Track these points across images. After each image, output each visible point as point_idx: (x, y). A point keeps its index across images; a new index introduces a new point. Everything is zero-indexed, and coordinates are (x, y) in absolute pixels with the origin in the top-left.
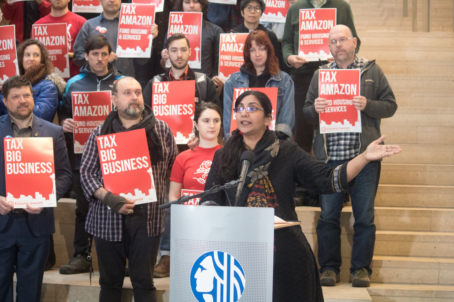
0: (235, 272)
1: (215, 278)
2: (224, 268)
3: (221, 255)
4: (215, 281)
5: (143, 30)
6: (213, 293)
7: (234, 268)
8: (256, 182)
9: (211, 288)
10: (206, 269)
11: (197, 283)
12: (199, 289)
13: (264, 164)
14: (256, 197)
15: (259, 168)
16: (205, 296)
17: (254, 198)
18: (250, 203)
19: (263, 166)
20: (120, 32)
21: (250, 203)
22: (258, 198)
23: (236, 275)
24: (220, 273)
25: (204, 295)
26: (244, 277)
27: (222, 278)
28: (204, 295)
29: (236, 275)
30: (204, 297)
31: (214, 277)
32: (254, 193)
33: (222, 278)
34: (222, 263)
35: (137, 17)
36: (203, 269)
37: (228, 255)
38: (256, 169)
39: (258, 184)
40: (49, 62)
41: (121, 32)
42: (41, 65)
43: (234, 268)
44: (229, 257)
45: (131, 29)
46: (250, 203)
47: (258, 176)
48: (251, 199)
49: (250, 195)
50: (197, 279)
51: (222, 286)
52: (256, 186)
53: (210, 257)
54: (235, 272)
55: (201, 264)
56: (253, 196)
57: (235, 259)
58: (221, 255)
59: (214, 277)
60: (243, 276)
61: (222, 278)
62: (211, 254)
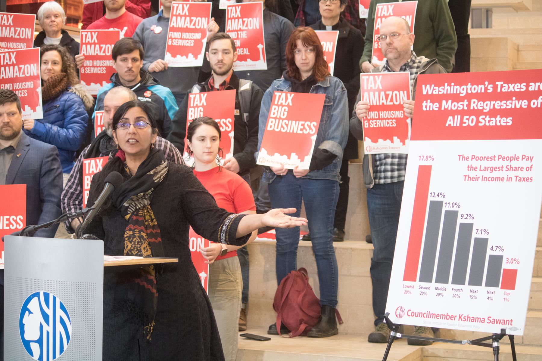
5: (196, 34)
8: (133, 212)
13: (145, 191)
14: (133, 231)
15: (137, 196)
17: (131, 233)
18: (127, 238)
19: (142, 194)
20: (170, 37)
21: (127, 238)
22: (136, 233)
32: (132, 226)
35: (242, 20)
38: (134, 197)
39: (137, 215)
40: (72, 71)
41: (171, 36)
42: (63, 74)
45: (183, 33)
46: (126, 239)
47: (136, 206)
48: (127, 233)
49: (127, 228)
52: (134, 218)
56: (130, 230)
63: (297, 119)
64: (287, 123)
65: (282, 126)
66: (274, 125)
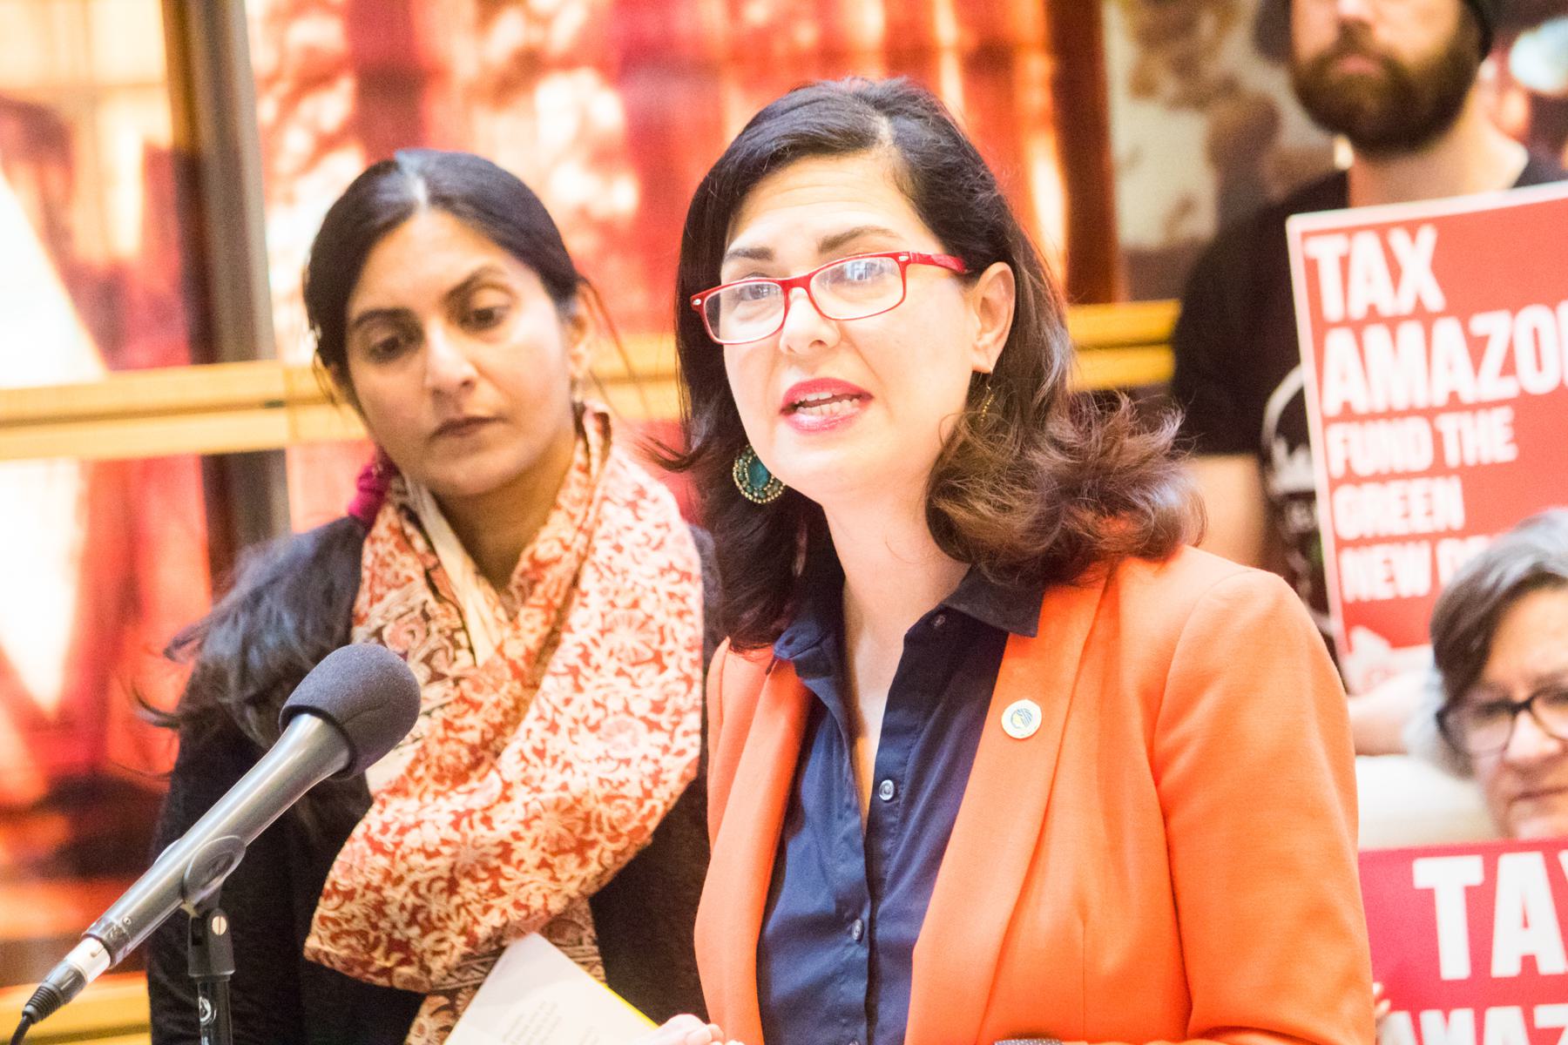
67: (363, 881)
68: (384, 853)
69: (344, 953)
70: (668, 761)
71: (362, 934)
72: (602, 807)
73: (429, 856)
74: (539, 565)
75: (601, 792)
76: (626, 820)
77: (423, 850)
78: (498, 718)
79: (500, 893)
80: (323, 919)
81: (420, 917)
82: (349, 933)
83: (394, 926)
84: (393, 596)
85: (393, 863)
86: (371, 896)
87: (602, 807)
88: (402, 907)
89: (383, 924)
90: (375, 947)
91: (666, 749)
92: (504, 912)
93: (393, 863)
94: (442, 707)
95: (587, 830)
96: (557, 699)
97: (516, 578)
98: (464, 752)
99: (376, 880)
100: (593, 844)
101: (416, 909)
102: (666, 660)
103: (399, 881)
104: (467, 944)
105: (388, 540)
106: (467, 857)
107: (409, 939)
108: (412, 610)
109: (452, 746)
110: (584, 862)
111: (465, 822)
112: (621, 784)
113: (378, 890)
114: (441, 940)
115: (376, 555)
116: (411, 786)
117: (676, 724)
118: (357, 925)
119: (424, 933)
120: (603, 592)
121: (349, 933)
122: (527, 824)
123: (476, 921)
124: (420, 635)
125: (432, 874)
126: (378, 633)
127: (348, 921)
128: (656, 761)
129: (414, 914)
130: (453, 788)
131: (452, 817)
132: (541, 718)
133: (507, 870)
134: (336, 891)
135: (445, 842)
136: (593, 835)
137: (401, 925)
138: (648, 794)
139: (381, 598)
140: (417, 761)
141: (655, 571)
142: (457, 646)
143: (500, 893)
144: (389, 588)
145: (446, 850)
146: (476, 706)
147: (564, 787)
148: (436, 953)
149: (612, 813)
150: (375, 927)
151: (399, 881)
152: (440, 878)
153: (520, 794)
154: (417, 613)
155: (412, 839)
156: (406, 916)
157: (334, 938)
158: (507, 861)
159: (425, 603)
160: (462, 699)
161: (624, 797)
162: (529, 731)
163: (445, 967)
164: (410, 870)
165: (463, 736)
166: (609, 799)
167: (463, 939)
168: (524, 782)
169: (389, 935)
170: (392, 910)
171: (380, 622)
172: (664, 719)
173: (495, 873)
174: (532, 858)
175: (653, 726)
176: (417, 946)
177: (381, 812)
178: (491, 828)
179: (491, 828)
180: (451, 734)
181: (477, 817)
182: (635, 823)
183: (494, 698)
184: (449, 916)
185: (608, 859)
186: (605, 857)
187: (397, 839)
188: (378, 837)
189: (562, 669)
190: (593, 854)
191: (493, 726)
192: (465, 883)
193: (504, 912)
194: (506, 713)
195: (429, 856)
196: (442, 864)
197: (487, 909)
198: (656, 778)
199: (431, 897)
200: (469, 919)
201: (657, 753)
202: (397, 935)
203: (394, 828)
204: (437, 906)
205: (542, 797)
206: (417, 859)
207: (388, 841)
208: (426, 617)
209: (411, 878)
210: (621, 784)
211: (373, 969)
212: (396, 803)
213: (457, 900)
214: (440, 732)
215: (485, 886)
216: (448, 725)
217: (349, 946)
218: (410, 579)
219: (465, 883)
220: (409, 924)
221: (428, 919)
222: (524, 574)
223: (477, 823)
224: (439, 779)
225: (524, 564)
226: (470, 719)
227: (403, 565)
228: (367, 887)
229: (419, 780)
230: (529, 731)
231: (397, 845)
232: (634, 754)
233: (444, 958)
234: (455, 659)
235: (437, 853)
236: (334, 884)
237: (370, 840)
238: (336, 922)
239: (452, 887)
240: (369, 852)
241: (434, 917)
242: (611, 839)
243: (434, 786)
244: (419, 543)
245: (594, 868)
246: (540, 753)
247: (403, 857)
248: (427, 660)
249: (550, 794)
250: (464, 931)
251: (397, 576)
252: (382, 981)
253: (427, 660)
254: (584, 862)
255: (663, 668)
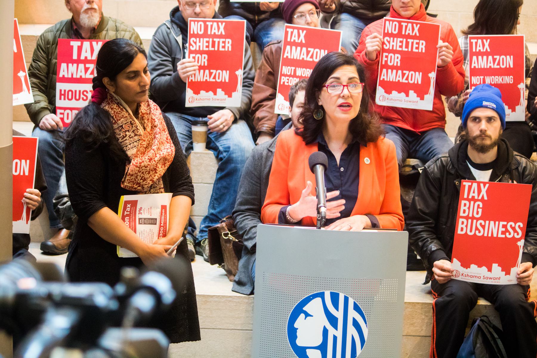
0: (354, 319)
1: (325, 327)
2: (339, 315)
3: (335, 298)
4: (325, 332)
6: (323, 348)
7: (352, 314)
9: (319, 341)
10: (312, 316)
11: (298, 334)
12: (300, 342)
16: (309, 352)
23: (356, 324)
24: (333, 321)
25: (308, 350)
26: (367, 326)
27: (336, 328)
28: (308, 350)
29: (356, 324)
30: (308, 354)
31: (325, 327)
33: (336, 328)
34: (336, 307)
36: (307, 315)
37: (345, 297)
43: (352, 314)
44: (346, 299)
50: (297, 329)
51: (335, 338)
53: (319, 300)
54: (354, 319)
55: (304, 309)
57: (354, 302)
58: (335, 298)
59: (325, 327)
60: (365, 325)
61: (335, 327)
62: (321, 295)
63: (496, 218)
64: (483, 223)
65: (477, 229)
66: (467, 226)
67: (134, 172)
68: (138, 167)
69: (130, 185)
70: (172, 148)
71: (133, 182)
72: (168, 157)
73: (146, 167)
74: (143, 114)
75: (167, 154)
76: (170, 159)
77: (144, 166)
78: (148, 143)
79: (157, 173)
80: (128, 180)
81: (143, 178)
82: (131, 182)
83: (138, 180)
84: (122, 119)
85: (140, 169)
86: (136, 175)
87: (168, 157)
88: (140, 176)
89: (137, 180)
90: (134, 184)
91: (171, 147)
92: (158, 176)
93: (140, 169)
94: (139, 140)
95: (165, 161)
96: (159, 138)
97: (140, 116)
98: (144, 149)
99: (137, 172)
100: (166, 163)
101: (143, 177)
102: (165, 130)
103: (140, 172)
104: (152, 182)
105: (118, 109)
106: (152, 167)
107: (140, 182)
108: (128, 122)
109: (142, 148)
110: (165, 167)
111: (151, 161)
112: (169, 152)
113: (137, 174)
114: (146, 182)
115: (115, 112)
116: (138, 156)
117: (170, 142)
118: (133, 180)
119: (143, 182)
120: (156, 118)
121: (131, 182)
122: (159, 161)
123: (153, 178)
124: (131, 127)
125: (146, 170)
126: (122, 126)
127: (131, 180)
128: (171, 148)
129: (142, 178)
130: (144, 155)
131: (148, 160)
132: (158, 142)
133: (157, 169)
134: (130, 175)
135: (149, 165)
136: (166, 162)
137: (139, 180)
138: (172, 154)
139: (120, 120)
140: (137, 151)
141: (159, 114)
142: (138, 129)
143: (157, 173)
144: (121, 118)
145: (149, 166)
146: (145, 141)
147: (163, 154)
148: (145, 185)
149: (168, 158)
150: (135, 180)
151: (140, 172)
152: (147, 171)
153: (158, 155)
154: (129, 123)
155: (143, 164)
156: (141, 178)
157: (129, 183)
158: (157, 167)
159: (131, 121)
160: (142, 139)
161: (169, 155)
162: (157, 144)
163: (148, 187)
164: (142, 170)
165: (144, 146)
166: (169, 155)
167: (151, 181)
168: (158, 153)
169: (137, 182)
170: (139, 177)
171: (121, 124)
172: (168, 141)
173: (155, 169)
174: (160, 167)
175: (168, 142)
176: (142, 184)
177: (134, 161)
178: (155, 162)
179: (155, 162)
180: (142, 146)
181: (153, 160)
182: (171, 159)
183: (147, 139)
184: (148, 178)
185: (168, 166)
186: (168, 165)
187: (140, 165)
188: (136, 165)
189: (158, 133)
190: (166, 165)
191: (148, 144)
192: (151, 172)
193: (158, 176)
194: (149, 141)
195: (146, 167)
196: (148, 168)
197: (155, 176)
198: (172, 150)
199: (145, 175)
200: (152, 178)
201: (170, 147)
202: (138, 182)
203: (139, 163)
204: (147, 176)
205: (161, 156)
206: (144, 168)
207: (138, 165)
208: (132, 124)
209: (142, 171)
210: (169, 152)
211: (133, 188)
212: (136, 159)
213: (150, 175)
214: (140, 146)
215: (154, 172)
216: (141, 144)
217: (131, 184)
218: (127, 117)
219: (151, 172)
220: (141, 180)
221: (144, 178)
222: (141, 115)
223: (153, 161)
224: (141, 154)
225: (141, 114)
226: (144, 143)
227: (124, 114)
228: (135, 173)
229: (139, 154)
230: (157, 144)
231: (140, 166)
232: (168, 147)
233: (147, 185)
234: (138, 132)
235: (147, 167)
236: (129, 173)
237: (133, 164)
238: (129, 180)
239: (149, 173)
240: (135, 167)
241: (146, 178)
242: (168, 162)
243: (141, 155)
244: (124, 110)
245: (166, 168)
246: (159, 148)
247: (141, 168)
248: (133, 131)
249: (162, 155)
250: (151, 180)
251: (123, 116)
252: (134, 190)
253: (133, 131)
254: (165, 167)
255: (165, 132)
